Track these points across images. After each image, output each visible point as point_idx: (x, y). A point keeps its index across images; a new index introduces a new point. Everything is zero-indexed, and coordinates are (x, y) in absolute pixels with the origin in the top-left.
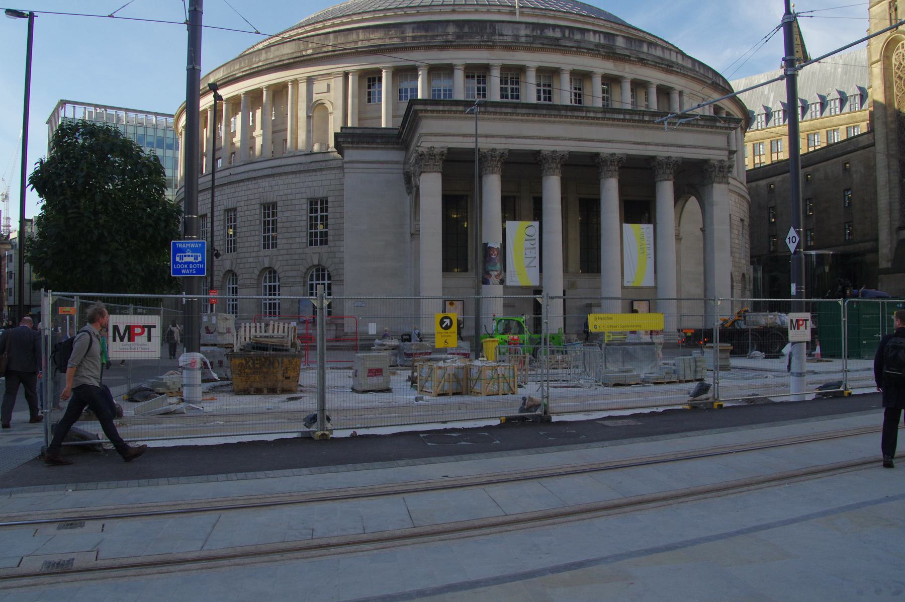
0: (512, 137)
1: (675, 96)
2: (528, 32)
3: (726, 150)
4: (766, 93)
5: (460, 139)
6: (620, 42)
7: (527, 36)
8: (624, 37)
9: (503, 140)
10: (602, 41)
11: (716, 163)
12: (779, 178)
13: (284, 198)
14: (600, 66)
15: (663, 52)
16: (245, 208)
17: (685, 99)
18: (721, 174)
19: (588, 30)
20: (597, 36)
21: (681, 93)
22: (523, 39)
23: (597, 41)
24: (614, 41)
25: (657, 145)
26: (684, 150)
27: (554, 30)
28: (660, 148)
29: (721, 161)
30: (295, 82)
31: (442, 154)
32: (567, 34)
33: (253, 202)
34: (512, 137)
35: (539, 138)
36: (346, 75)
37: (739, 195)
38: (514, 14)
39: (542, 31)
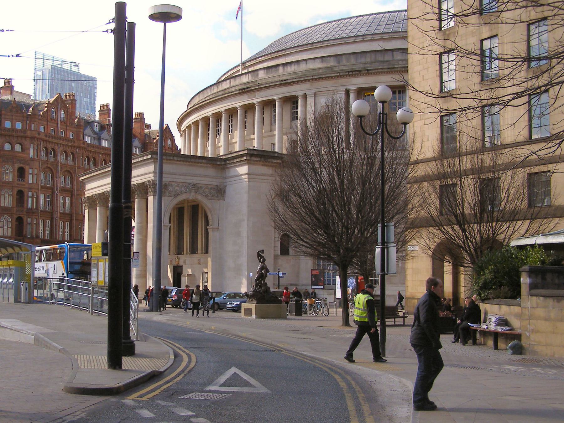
6: (262, 74)
8: (264, 69)
17: (310, 100)
21: (305, 97)
24: (258, 74)
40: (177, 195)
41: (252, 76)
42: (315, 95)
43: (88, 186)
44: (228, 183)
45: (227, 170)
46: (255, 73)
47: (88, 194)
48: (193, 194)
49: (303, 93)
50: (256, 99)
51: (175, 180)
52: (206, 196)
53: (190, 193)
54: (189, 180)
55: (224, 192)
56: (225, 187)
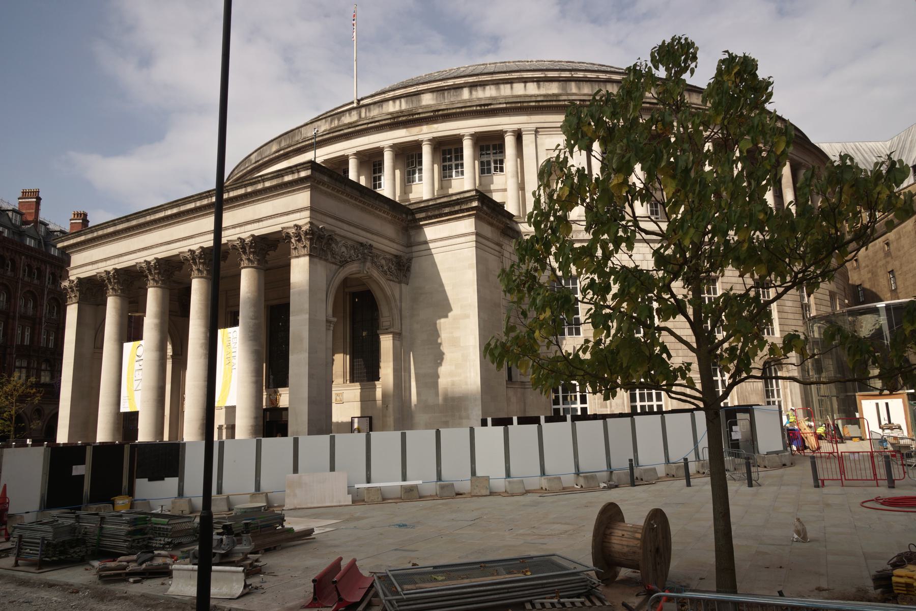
1: (509, 141)
5: (90, 267)
9: (116, 260)
11: (292, 231)
15: (498, 89)
17: (528, 140)
18: (300, 245)
19: (387, 100)
20: (398, 102)
21: (518, 136)
23: (397, 108)
24: (419, 101)
26: (261, 224)
27: (350, 114)
29: (298, 227)
32: (363, 115)
39: (339, 120)
40: (343, 263)
41: (407, 102)
42: (537, 131)
43: (77, 259)
44: (415, 254)
45: (412, 233)
46: (414, 98)
47: (74, 275)
48: (368, 264)
49: (516, 127)
50: (425, 133)
51: (343, 233)
52: (385, 273)
53: (364, 262)
54: (363, 237)
55: (408, 269)
56: (410, 260)
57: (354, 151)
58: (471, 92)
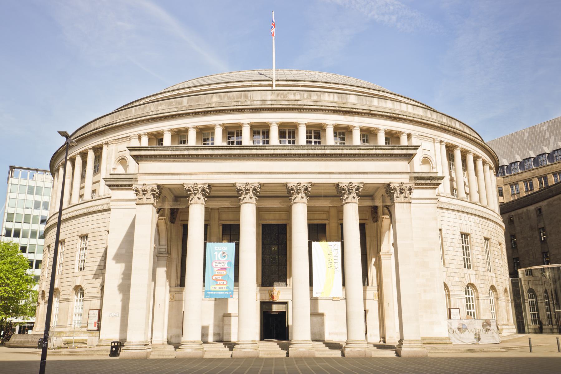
0: (212, 173)
2: (274, 97)
3: (407, 173)
4: (547, 136)
7: (271, 100)
9: (205, 176)
10: (336, 99)
11: (397, 186)
12: (545, 203)
13: (92, 231)
14: (331, 120)
16: (69, 240)
22: (269, 103)
23: (331, 99)
25: (340, 173)
27: (295, 95)
28: (343, 176)
30: (107, 143)
31: (153, 190)
33: (74, 234)
34: (212, 173)
35: (235, 173)
36: (140, 137)
37: (480, 217)
38: (272, 86)
41: (338, 98)
49: (409, 132)
57: (307, 121)
58: (379, 103)
